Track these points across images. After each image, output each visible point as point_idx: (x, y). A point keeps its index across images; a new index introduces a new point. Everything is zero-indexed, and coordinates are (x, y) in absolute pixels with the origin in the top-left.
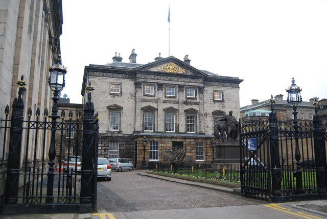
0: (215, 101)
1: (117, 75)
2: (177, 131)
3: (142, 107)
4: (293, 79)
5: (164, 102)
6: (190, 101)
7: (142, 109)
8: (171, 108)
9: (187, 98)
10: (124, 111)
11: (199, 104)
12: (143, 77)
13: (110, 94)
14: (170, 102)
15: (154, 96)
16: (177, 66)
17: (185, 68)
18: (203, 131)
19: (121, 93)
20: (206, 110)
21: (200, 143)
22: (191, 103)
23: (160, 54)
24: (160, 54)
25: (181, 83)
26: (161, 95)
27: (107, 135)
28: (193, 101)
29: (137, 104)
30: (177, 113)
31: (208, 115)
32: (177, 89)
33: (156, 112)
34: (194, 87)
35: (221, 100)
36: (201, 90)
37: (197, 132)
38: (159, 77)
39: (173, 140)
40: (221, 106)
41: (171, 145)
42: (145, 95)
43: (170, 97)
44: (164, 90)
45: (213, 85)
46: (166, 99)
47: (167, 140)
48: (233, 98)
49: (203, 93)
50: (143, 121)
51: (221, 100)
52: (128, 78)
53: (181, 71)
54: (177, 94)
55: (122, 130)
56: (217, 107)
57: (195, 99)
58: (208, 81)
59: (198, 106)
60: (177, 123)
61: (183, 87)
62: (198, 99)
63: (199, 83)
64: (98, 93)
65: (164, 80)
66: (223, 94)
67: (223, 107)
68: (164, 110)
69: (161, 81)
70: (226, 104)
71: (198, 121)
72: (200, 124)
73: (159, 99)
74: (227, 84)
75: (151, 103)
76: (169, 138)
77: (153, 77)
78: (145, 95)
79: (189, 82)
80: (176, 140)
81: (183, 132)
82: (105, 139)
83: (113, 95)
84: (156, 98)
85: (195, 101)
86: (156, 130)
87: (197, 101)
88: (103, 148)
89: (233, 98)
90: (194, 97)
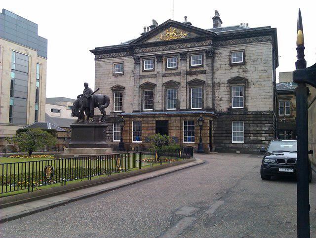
0: (231, 65)
2: (179, 109)
5: (164, 76)
6: (194, 70)
8: (171, 81)
9: (191, 67)
10: (127, 90)
12: (141, 51)
13: (114, 75)
14: (171, 75)
16: (178, 30)
18: (211, 105)
19: (123, 72)
21: (189, 121)
22: (195, 73)
23: (186, 18)
24: (186, 18)
25: (182, 51)
26: (159, 68)
28: (199, 69)
32: (179, 58)
34: (200, 52)
36: (211, 55)
39: (157, 119)
40: (241, 70)
41: (155, 125)
42: (144, 71)
46: (167, 72)
47: (150, 119)
48: (260, 57)
50: (142, 100)
52: (130, 55)
54: (179, 64)
55: (124, 110)
56: (235, 73)
57: (202, 66)
58: (222, 40)
59: (204, 75)
62: (205, 66)
65: (164, 50)
66: (244, 54)
70: (248, 67)
71: (205, 94)
72: (207, 98)
73: (158, 72)
74: (252, 39)
75: (150, 79)
76: (151, 117)
77: (151, 49)
78: (144, 71)
79: (193, 47)
80: (160, 119)
84: (155, 73)
85: (202, 69)
87: (204, 69)
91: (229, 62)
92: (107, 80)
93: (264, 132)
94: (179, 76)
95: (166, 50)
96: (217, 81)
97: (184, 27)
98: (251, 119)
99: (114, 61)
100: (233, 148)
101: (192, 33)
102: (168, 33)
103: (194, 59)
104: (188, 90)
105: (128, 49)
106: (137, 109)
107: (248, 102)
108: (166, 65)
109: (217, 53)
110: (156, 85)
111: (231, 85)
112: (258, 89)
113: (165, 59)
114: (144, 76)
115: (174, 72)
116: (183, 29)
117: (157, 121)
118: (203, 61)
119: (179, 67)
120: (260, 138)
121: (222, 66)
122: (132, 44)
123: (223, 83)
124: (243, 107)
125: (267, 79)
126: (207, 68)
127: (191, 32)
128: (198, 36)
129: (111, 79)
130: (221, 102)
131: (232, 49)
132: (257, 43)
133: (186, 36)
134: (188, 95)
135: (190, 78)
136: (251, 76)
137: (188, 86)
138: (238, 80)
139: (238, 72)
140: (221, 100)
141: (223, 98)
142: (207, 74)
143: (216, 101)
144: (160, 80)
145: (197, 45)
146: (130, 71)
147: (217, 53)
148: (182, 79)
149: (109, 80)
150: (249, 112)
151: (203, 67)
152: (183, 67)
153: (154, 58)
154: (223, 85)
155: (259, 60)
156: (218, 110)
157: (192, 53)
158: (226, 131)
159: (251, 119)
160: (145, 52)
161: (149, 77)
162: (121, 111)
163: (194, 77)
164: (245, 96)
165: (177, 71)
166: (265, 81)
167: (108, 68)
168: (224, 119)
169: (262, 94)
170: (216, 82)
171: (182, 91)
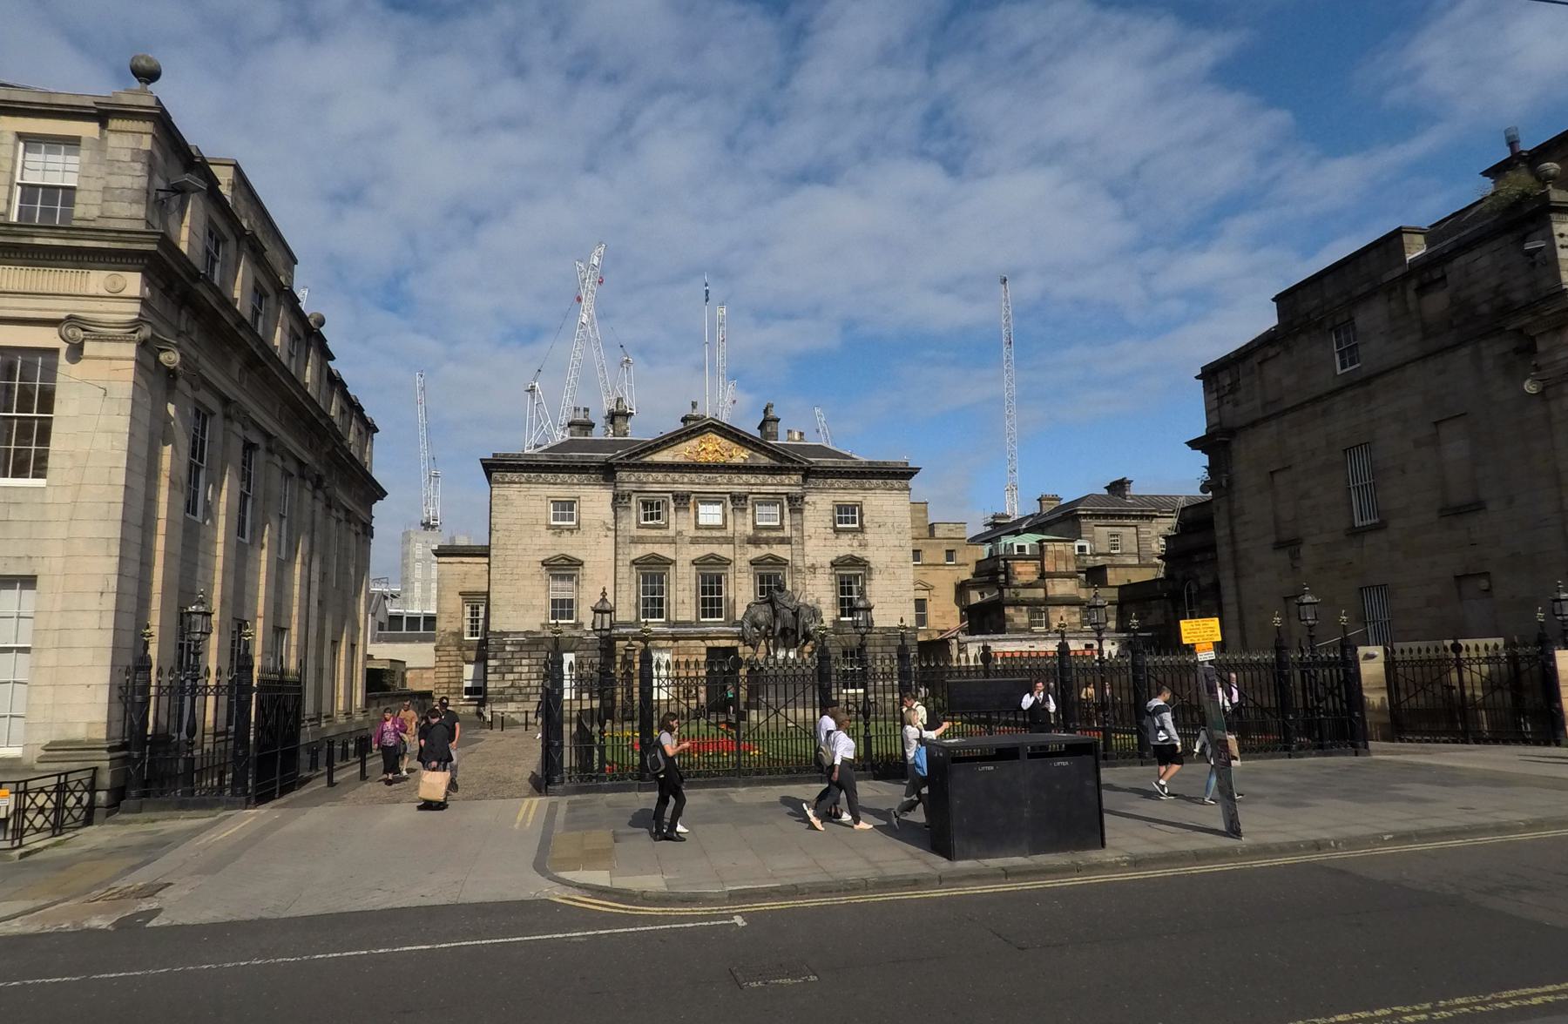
3: (633, 558)
4: (604, 589)
5: (695, 541)
7: (633, 562)
8: (712, 556)
9: (756, 527)
10: (588, 569)
11: (790, 543)
12: (633, 479)
13: (549, 527)
19: (578, 523)
20: (814, 557)
22: (767, 542)
25: (737, 489)
27: (542, 636)
28: (774, 534)
29: (620, 551)
30: (730, 569)
31: (819, 571)
35: (857, 525)
36: (796, 504)
38: (677, 476)
39: (709, 643)
40: (856, 543)
44: (692, 510)
45: (831, 487)
46: (699, 533)
47: (692, 643)
48: (891, 520)
49: (801, 511)
50: (638, 596)
51: (857, 525)
53: (740, 455)
54: (730, 517)
56: (845, 546)
59: (788, 547)
60: (731, 595)
61: (746, 498)
62: (787, 528)
63: (789, 485)
65: (692, 483)
67: (863, 545)
68: (693, 563)
69: (684, 483)
70: (867, 537)
73: (679, 533)
77: (660, 476)
78: (639, 527)
79: (763, 485)
80: (717, 643)
83: (558, 530)
84: (671, 532)
85: (781, 534)
86: (672, 618)
87: (787, 532)
89: (890, 520)
90: (778, 523)
92: (530, 542)
95: (699, 484)
96: (809, 561)
98: (878, 642)
99: (549, 494)
101: (757, 455)
102: (704, 446)
106: (626, 619)
108: (697, 517)
110: (673, 562)
111: (837, 572)
112: (889, 582)
113: (695, 502)
114: (642, 537)
115: (716, 534)
117: (709, 649)
118: (782, 518)
119: (728, 523)
122: (613, 461)
123: (822, 567)
125: (904, 564)
126: (794, 533)
128: (772, 461)
129: (541, 539)
131: (837, 499)
132: (883, 491)
133: (745, 459)
135: (755, 553)
136: (874, 556)
139: (851, 546)
142: (793, 547)
144: (684, 550)
145: (770, 481)
146: (597, 524)
147: (807, 503)
149: (537, 541)
150: (876, 628)
151: (783, 529)
152: (743, 525)
153: (666, 497)
154: (822, 570)
155: (889, 525)
159: (878, 642)
160: (645, 483)
161: (655, 541)
162: (573, 621)
163: (764, 551)
166: (901, 567)
167: (532, 510)
169: (899, 594)
170: (808, 564)
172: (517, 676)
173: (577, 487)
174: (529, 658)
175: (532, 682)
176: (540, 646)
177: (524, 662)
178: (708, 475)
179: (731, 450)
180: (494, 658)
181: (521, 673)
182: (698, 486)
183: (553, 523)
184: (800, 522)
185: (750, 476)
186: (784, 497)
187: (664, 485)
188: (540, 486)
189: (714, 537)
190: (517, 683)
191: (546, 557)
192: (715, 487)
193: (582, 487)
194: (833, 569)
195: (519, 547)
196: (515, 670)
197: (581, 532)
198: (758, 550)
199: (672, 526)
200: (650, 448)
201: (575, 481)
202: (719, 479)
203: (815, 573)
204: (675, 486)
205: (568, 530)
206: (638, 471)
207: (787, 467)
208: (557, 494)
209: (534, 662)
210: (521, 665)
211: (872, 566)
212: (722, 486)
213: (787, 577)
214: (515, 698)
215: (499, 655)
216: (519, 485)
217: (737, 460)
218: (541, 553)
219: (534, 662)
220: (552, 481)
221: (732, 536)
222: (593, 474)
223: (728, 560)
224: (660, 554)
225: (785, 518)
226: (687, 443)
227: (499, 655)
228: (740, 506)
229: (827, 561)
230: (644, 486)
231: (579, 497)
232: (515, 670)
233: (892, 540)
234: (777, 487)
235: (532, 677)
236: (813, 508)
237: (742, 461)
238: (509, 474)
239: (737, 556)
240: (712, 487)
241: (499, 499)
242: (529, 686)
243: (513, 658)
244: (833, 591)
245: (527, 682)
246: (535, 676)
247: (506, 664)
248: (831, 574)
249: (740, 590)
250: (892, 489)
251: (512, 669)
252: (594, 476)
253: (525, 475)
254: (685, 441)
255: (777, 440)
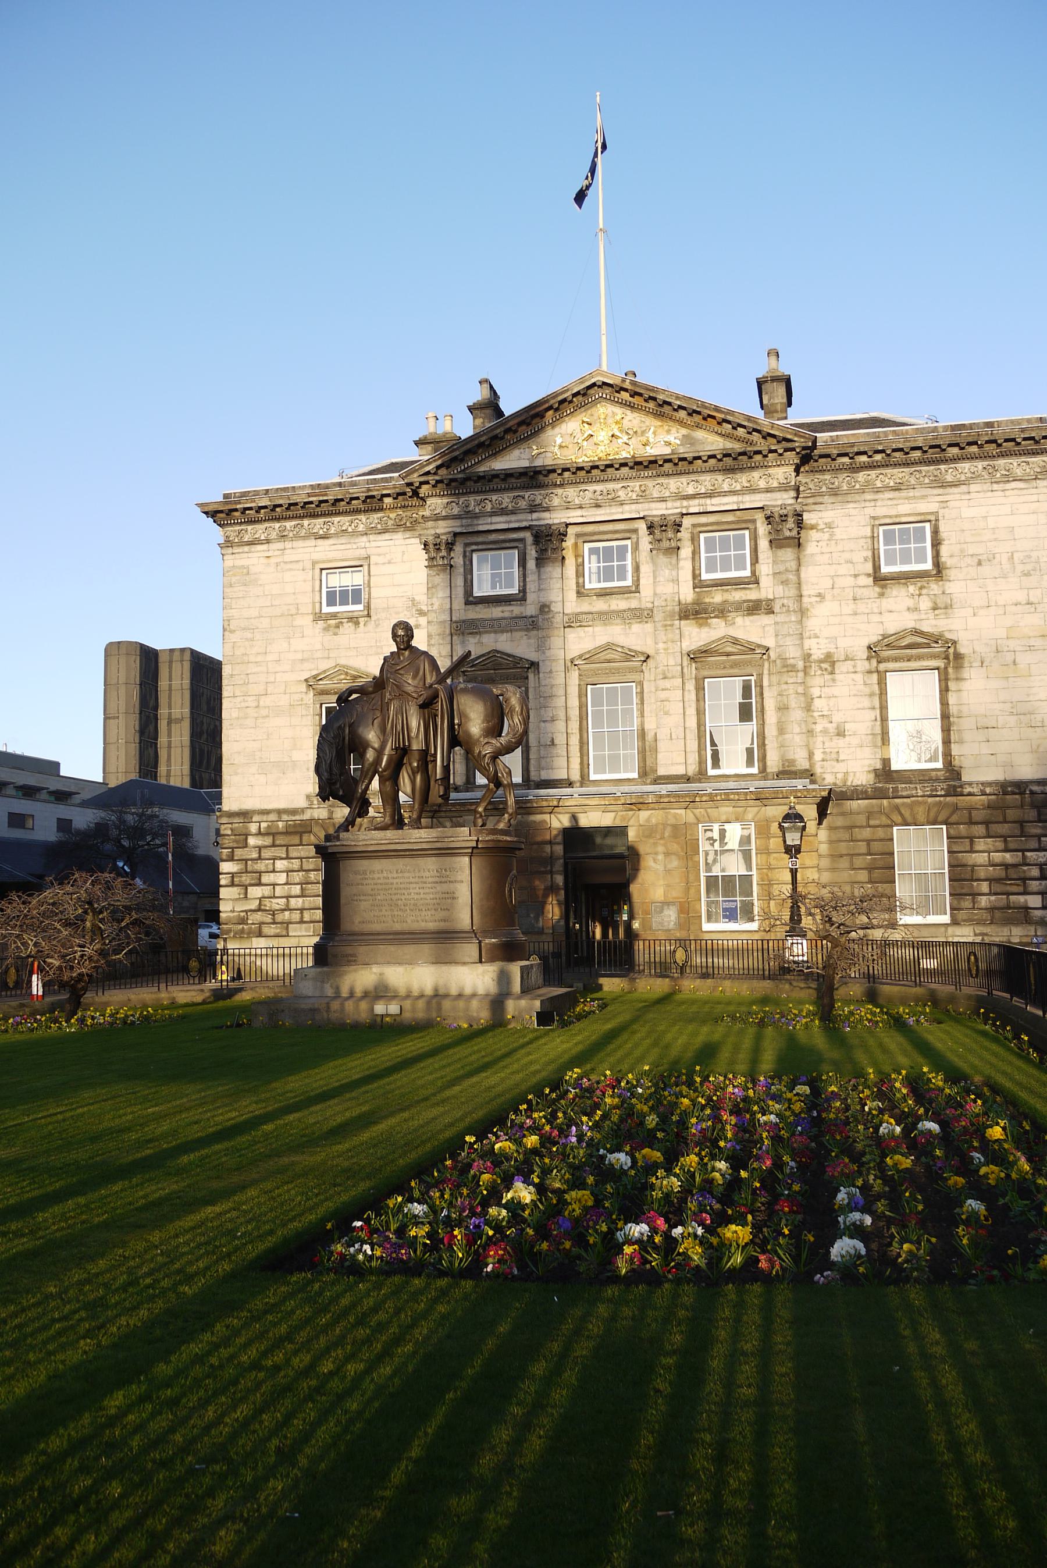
1: (342, 522)
6: (717, 597)
8: (609, 647)
9: (698, 584)
11: (770, 611)
14: (605, 617)
15: (521, 597)
16: (633, 419)
17: (681, 423)
19: (368, 607)
20: (834, 639)
22: (722, 611)
25: (657, 510)
27: (307, 816)
31: (841, 667)
33: (531, 676)
34: (742, 519)
37: (763, 769)
40: (925, 604)
42: (471, 600)
43: (603, 594)
45: (868, 487)
46: (585, 606)
51: (928, 566)
52: (399, 526)
54: (645, 569)
60: (650, 725)
61: (678, 526)
62: (765, 581)
63: (768, 490)
64: (265, 623)
66: (935, 532)
70: (955, 586)
74: (965, 466)
75: (504, 637)
77: (506, 499)
79: (710, 495)
81: (680, 770)
82: (301, 834)
83: (331, 622)
85: (752, 594)
86: (534, 776)
88: (297, 877)
90: (747, 573)
91: (869, 568)
93: (1035, 872)
94: (649, 627)
97: (669, 404)
99: (316, 556)
100: (904, 944)
101: (700, 434)
103: (710, 546)
104: (691, 686)
105: (387, 500)
107: (961, 742)
108: (580, 573)
109: (813, 527)
110: (534, 665)
111: (882, 667)
113: (576, 544)
116: (659, 415)
118: (755, 560)
119: (642, 581)
120: (1022, 899)
121: (840, 582)
124: (939, 765)
126: (780, 591)
127: (698, 426)
130: (841, 742)
131: (880, 511)
132: (987, 486)
134: (692, 711)
137: (691, 670)
138: (909, 646)
139: (916, 609)
140: (841, 733)
141: (847, 726)
142: (780, 618)
143: (820, 739)
147: (813, 527)
148: (662, 636)
150: (970, 784)
153: (522, 540)
154: (848, 665)
156: (829, 780)
157: (703, 519)
158: (870, 869)
160: (476, 516)
161: (496, 626)
163: (715, 631)
164: (945, 716)
165: (634, 604)
166: (1030, 648)
168: (861, 820)
170: (817, 654)
171: (663, 695)
172: (267, 891)
173: (364, 538)
174: (287, 858)
175: (293, 901)
176: (305, 837)
177: (280, 865)
178: (598, 487)
179: (643, 433)
180: (231, 858)
181: (274, 885)
182: (579, 512)
183: (326, 609)
184: (793, 565)
185: (684, 479)
186: (760, 517)
187: (513, 518)
188: (300, 543)
189: (614, 611)
190: (268, 904)
191: (314, 673)
192: (614, 510)
193: (372, 537)
194: (874, 662)
195: (269, 657)
196: (265, 879)
197: (371, 624)
198: (705, 630)
199: (531, 597)
200: (481, 445)
201: (361, 528)
202: (622, 494)
203: (832, 673)
204: (535, 516)
205: (350, 619)
206: (463, 494)
207: (759, 452)
208: (331, 555)
209: (296, 864)
210: (274, 871)
211: (962, 650)
212: (626, 507)
213: (765, 683)
214: (266, 930)
215: (239, 853)
216: (265, 547)
217: (657, 449)
218: (307, 665)
219: (296, 864)
220: (321, 532)
221: (650, 605)
222: (393, 508)
223: (643, 653)
224: (509, 650)
225: (760, 561)
226: (557, 430)
227: (239, 853)
228: (665, 544)
229: (858, 646)
230: (476, 522)
231: (368, 558)
232: (265, 879)
233: (1011, 592)
234: (740, 498)
235: (293, 893)
236: (826, 536)
237: (667, 451)
238: (250, 528)
239: (661, 646)
240: (608, 510)
241: (235, 575)
242: (288, 909)
243: (260, 858)
244: (874, 708)
245: (284, 900)
246: (296, 890)
247: (249, 869)
248: (870, 672)
249: (666, 713)
250: (1009, 478)
251: (260, 879)
252: (393, 515)
253: (277, 525)
254: (553, 425)
255: (786, 418)
